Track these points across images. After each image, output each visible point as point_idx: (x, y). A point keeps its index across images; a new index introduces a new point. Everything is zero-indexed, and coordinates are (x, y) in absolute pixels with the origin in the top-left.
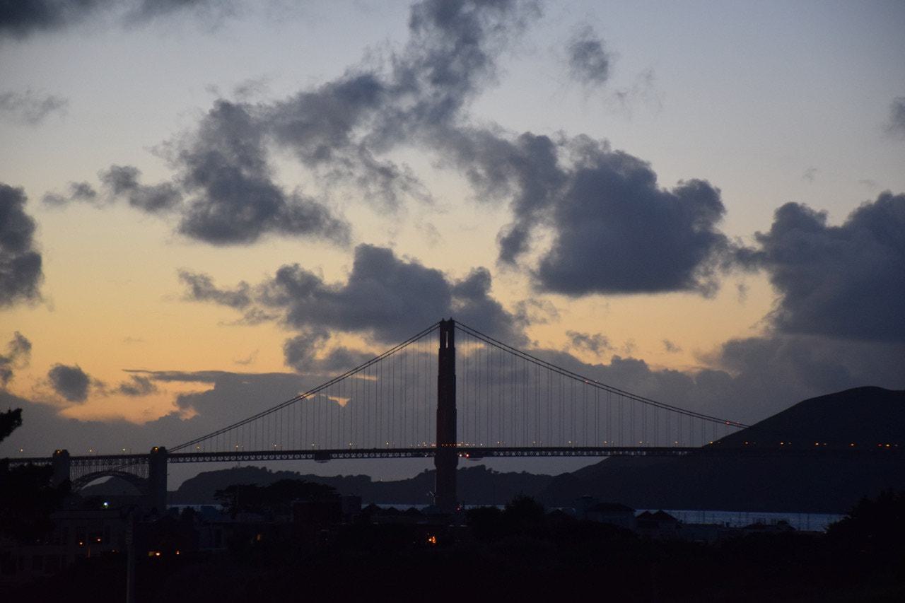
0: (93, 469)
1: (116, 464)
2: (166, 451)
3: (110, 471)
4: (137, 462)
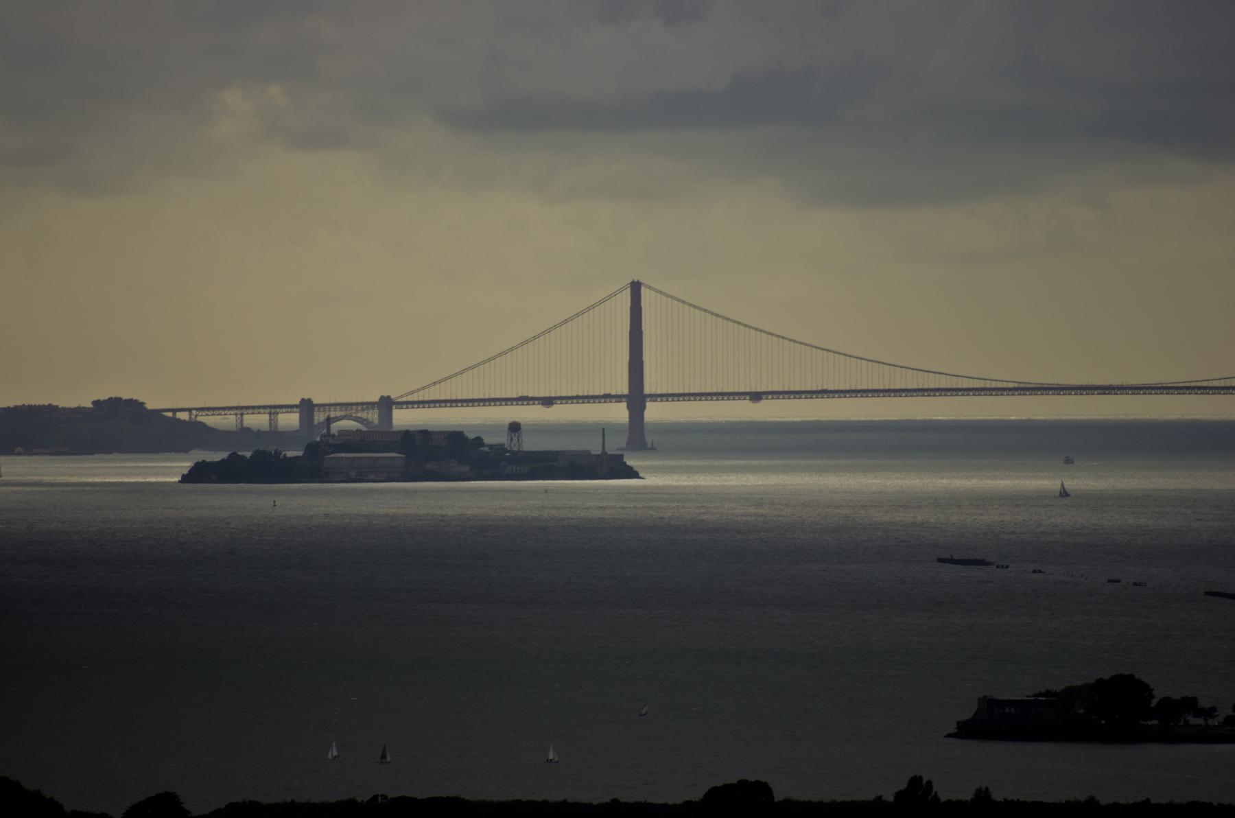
1: (350, 410)
2: (391, 399)
3: (345, 416)
4: (368, 409)
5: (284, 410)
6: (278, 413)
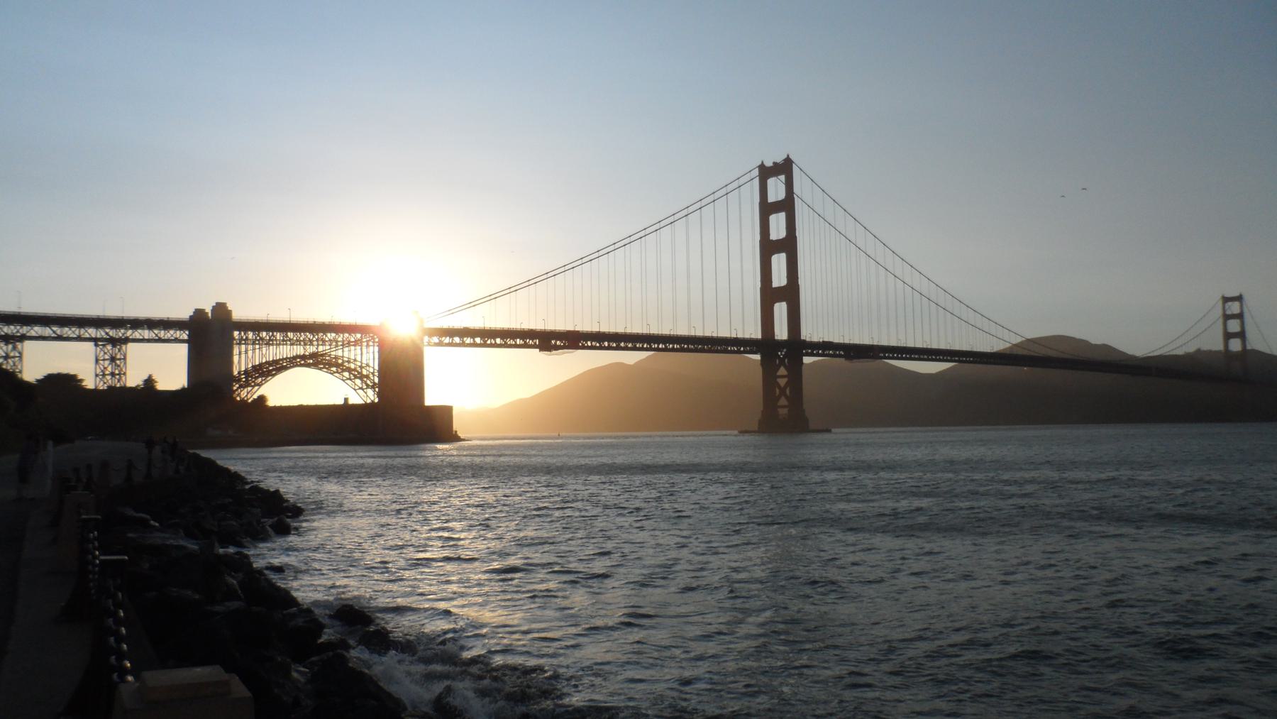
0: (286, 351)
5: (146, 334)
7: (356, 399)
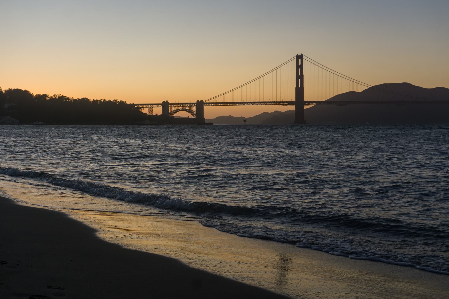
4: (192, 106)
5: (155, 106)
6: (153, 107)
7: (191, 116)
